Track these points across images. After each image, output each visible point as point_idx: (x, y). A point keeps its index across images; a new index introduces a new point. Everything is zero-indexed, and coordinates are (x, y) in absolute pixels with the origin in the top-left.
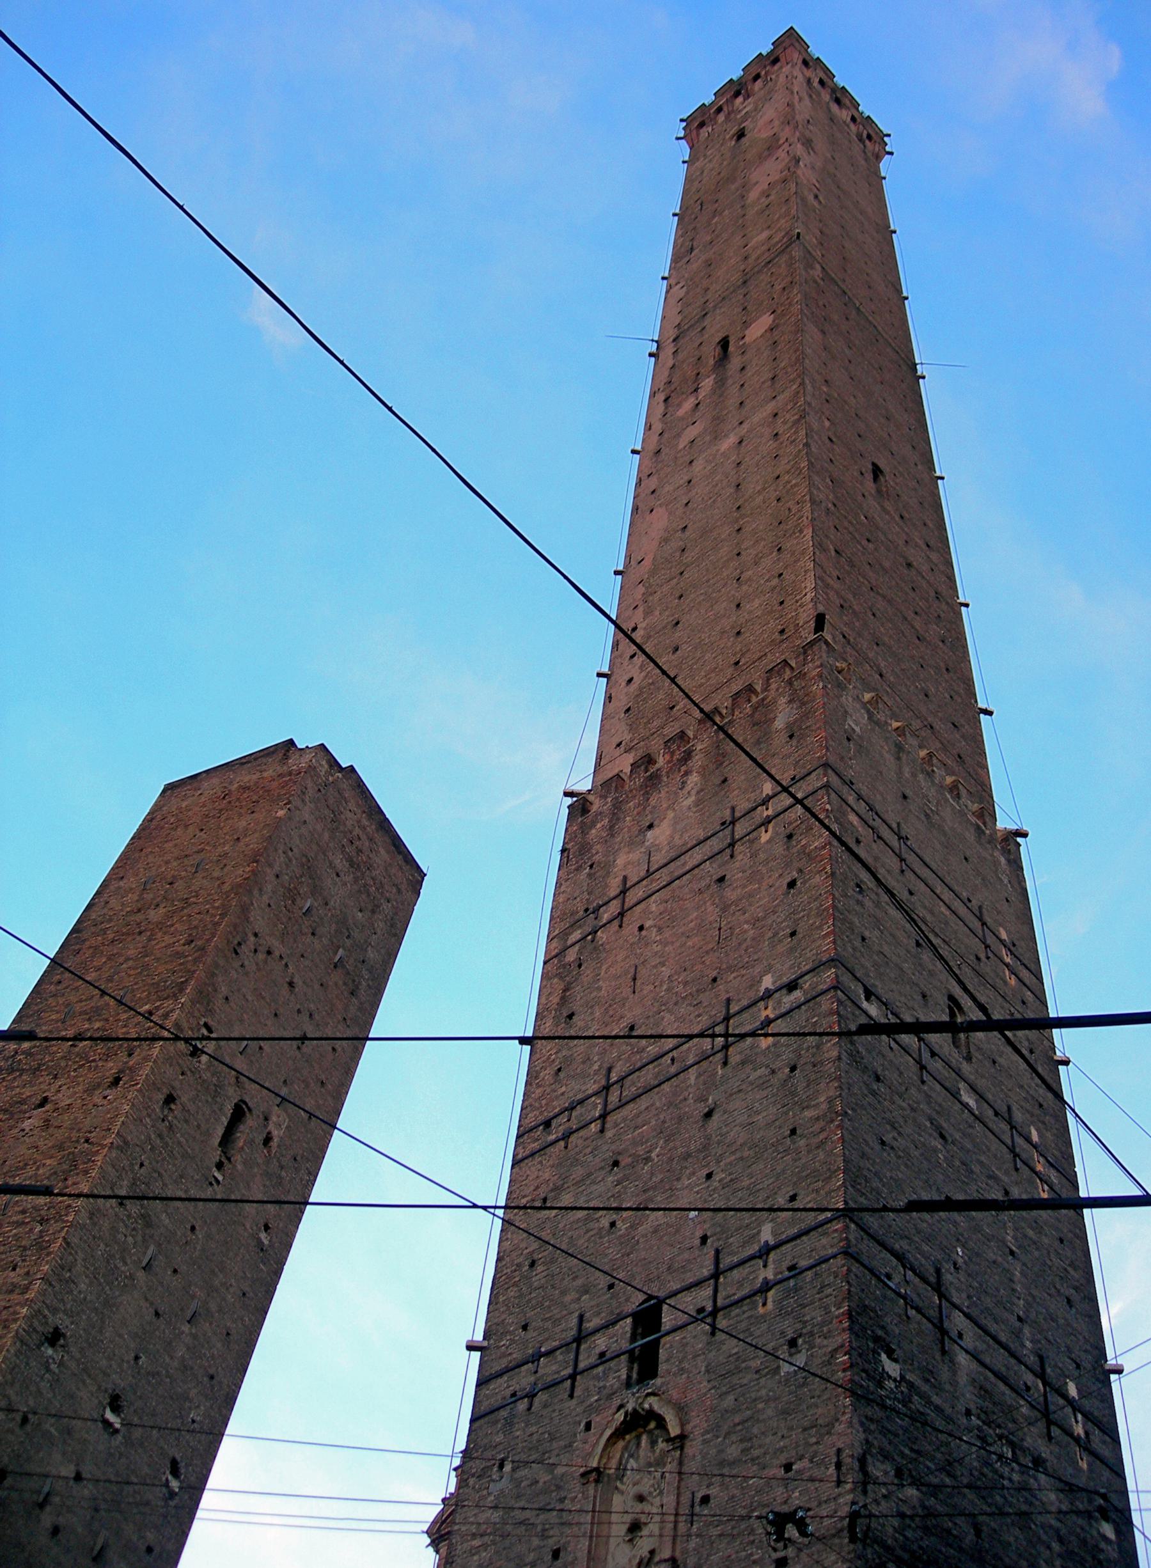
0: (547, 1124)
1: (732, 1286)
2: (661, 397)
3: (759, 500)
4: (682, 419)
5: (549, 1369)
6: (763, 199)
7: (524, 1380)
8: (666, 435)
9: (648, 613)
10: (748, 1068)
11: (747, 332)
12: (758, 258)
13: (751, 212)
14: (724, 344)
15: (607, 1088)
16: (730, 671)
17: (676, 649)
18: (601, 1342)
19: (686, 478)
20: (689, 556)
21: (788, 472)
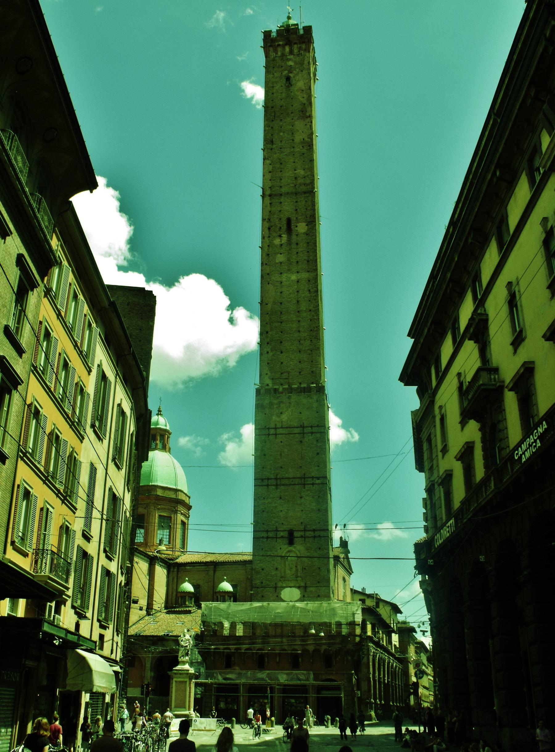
0: (262, 480)
1: (308, 534)
2: (267, 225)
3: (305, 314)
4: (276, 246)
5: (271, 535)
6: (301, 148)
7: (265, 534)
8: (271, 249)
9: (271, 330)
10: (309, 492)
11: (298, 225)
12: (300, 185)
13: (297, 150)
14: (289, 221)
15: (276, 479)
16: (298, 374)
17: (282, 352)
18: (282, 534)
19: (279, 280)
20: (284, 317)
21: (314, 311)
